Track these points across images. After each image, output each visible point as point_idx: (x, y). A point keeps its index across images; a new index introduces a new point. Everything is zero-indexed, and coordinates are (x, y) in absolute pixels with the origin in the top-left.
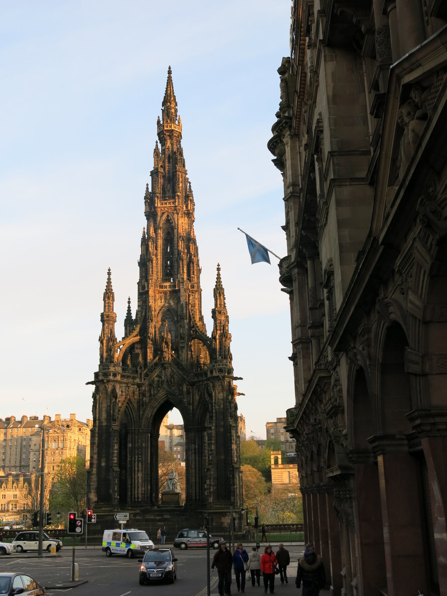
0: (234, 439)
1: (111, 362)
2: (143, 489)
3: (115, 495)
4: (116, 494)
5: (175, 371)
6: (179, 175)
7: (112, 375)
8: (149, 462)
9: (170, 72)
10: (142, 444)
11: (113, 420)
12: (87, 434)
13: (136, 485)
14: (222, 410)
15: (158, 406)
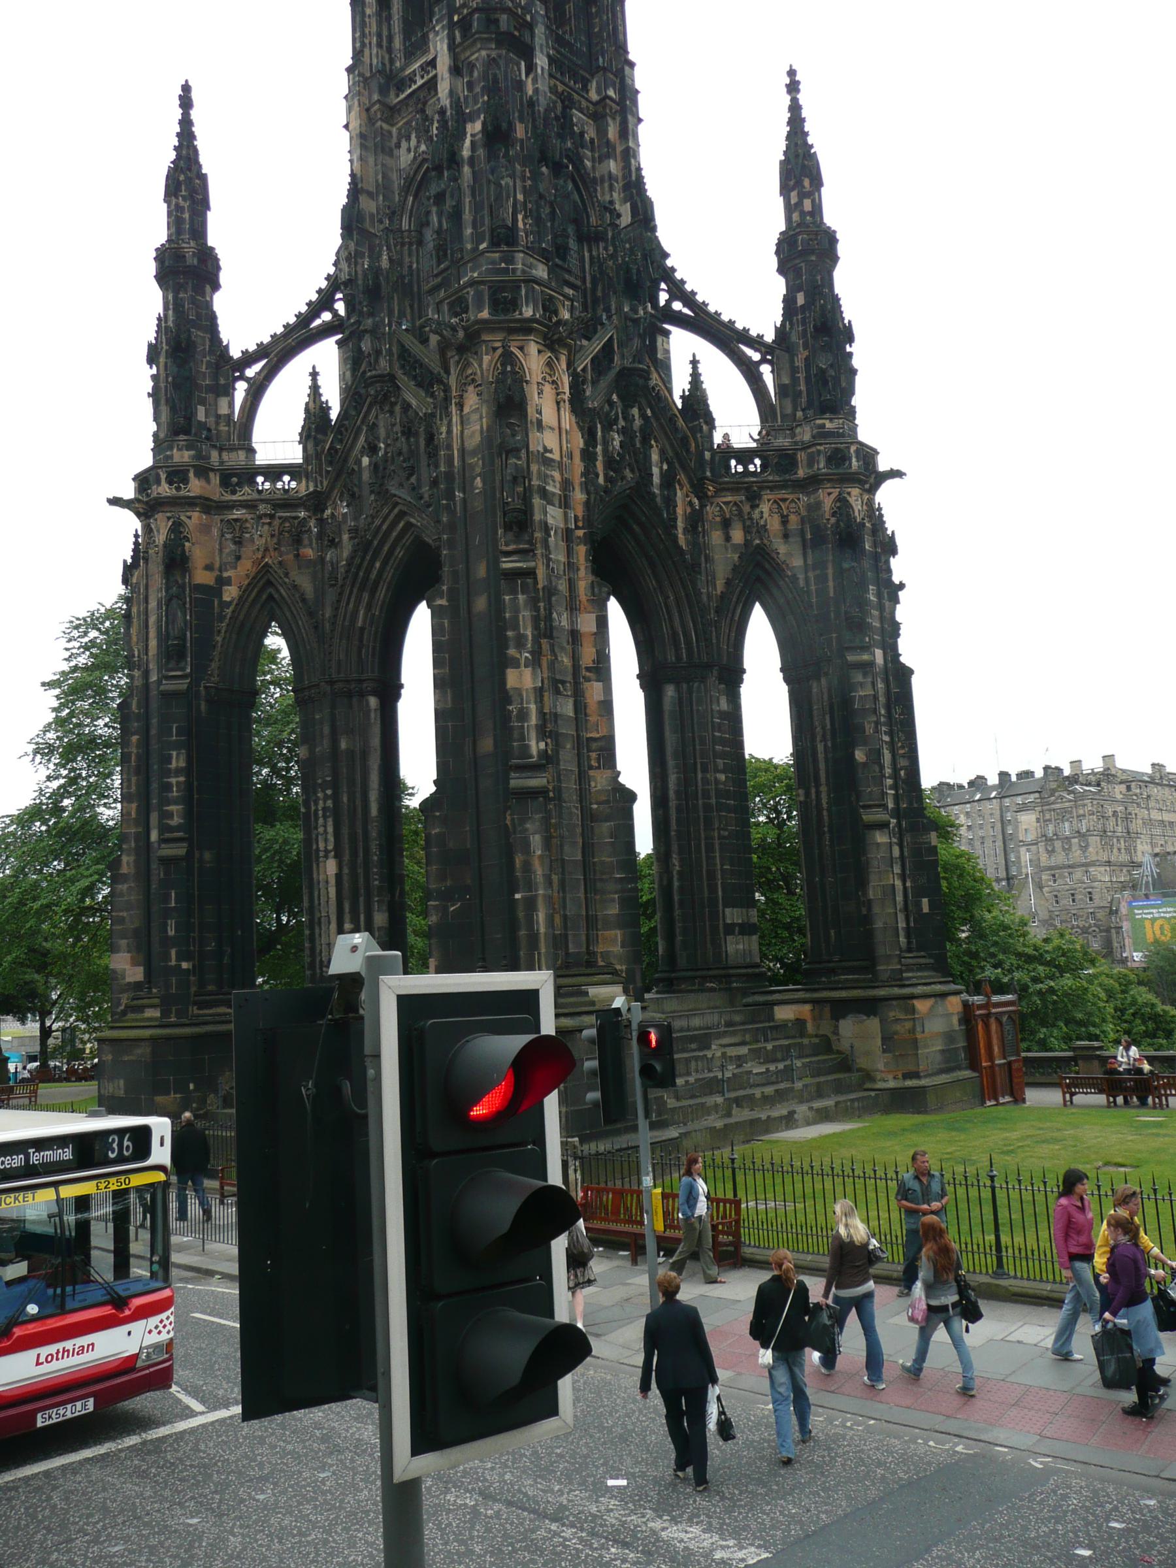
0: (520, 642)
3: (167, 958)
4: (173, 952)
5: (414, 403)
7: (163, 476)
8: (374, 811)
10: (335, 742)
12: (1149, 797)
14: (478, 505)
15: (389, 575)
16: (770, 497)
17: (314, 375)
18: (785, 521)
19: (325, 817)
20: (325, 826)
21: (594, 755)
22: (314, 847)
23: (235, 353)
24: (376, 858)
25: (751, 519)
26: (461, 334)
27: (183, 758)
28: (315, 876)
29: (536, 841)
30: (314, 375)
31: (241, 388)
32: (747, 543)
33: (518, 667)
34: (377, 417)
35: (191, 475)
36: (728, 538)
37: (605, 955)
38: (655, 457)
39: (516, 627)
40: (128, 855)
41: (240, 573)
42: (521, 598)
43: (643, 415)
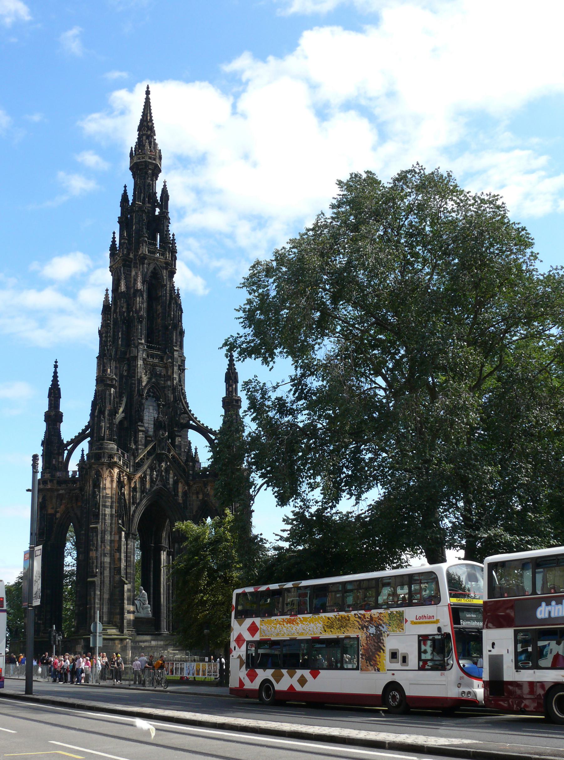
17: (83, 451)
23: (65, 442)
30: (83, 451)
31: (66, 452)
32: (203, 499)
36: (198, 497)
37: (115, 622)
38: (171, 476)
39: (93, 541)
41: (61, 509)
42: (94, 534)
43: (166, 464)
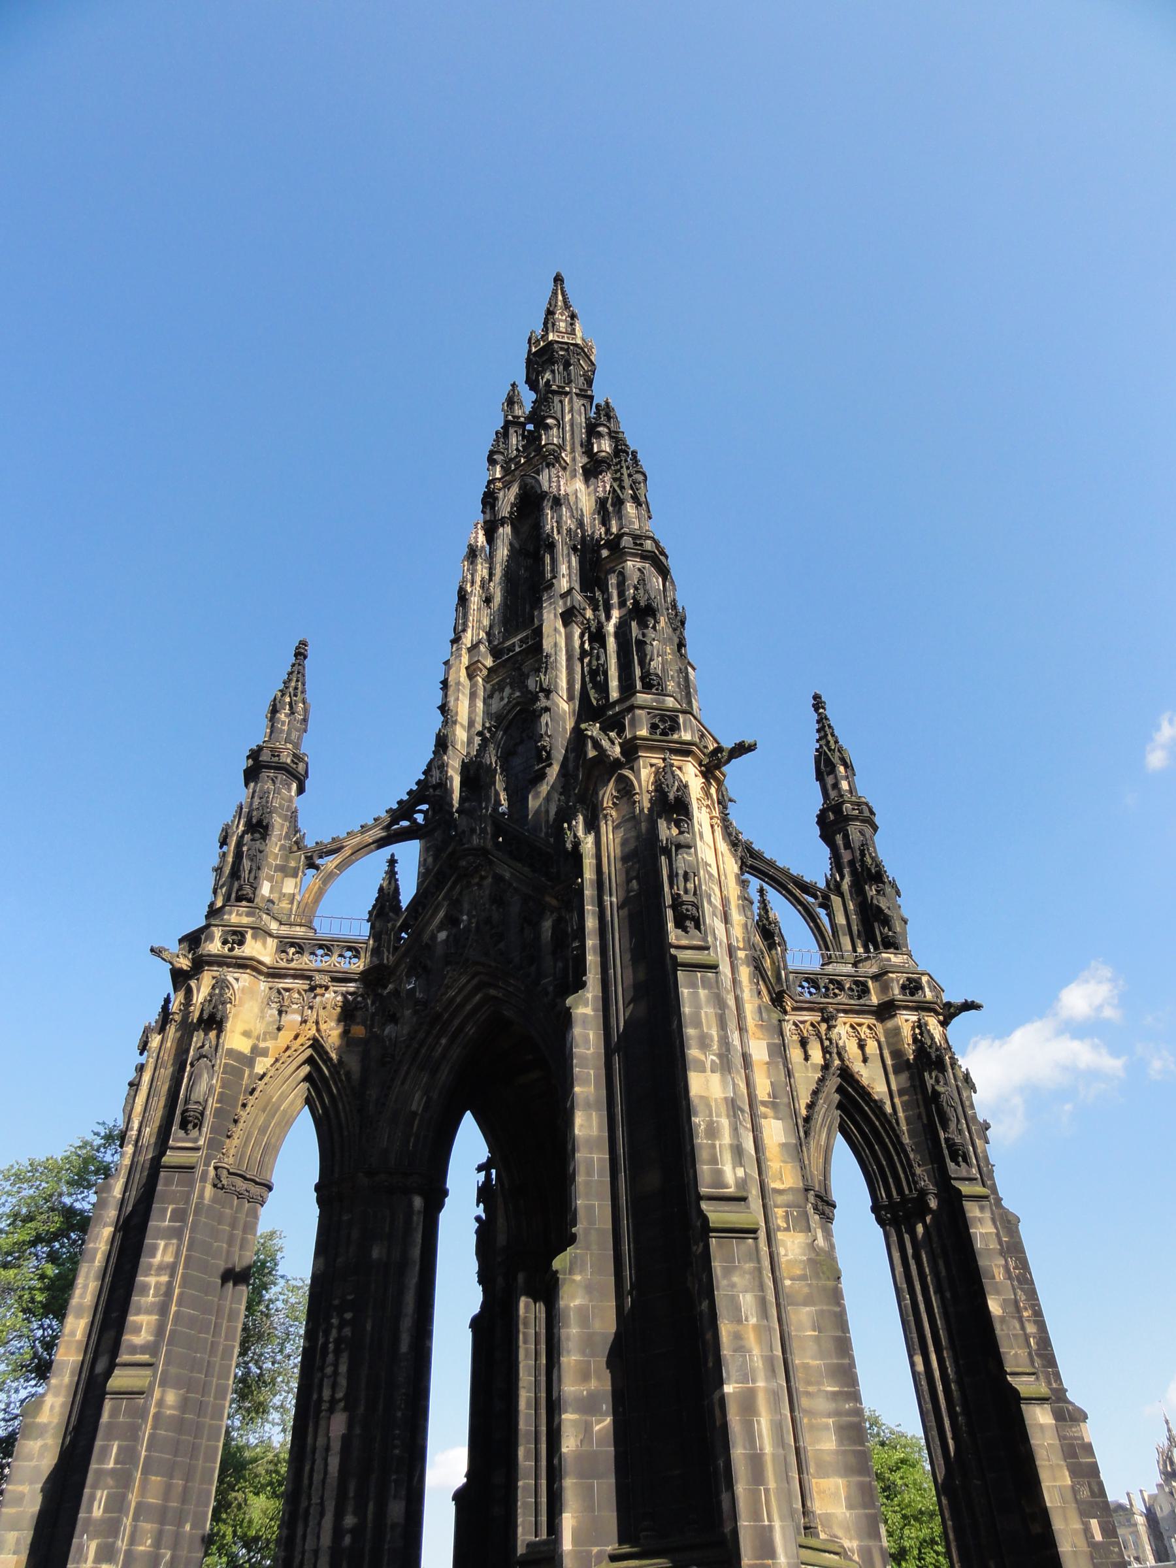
1: (239, 899)
2: (349, 1521)
5: (507, 875)
6: (561, 402)
9: (558, 279)
11: (184, 1125)
13: (315, 1500)
16: (845, 1020)
17: (392, 862)
18: (862, 1046)
19: (337, 1352)
20: (336, 1365)
21: (780, 1212)
22: (315, 1396)
24: (399, 1414)
25: (830, 1040)
26: (618, 749)
27: (172, 1249)
28: (310, 1440)
29: (747, 1301)
30: (392, 862)
33: (704, 1071)
34: (460, 893)
35: (249, 936)
36: (807, 1058)
39: (698, 1024)
40: (56, 1395)
42: (703, 993)
